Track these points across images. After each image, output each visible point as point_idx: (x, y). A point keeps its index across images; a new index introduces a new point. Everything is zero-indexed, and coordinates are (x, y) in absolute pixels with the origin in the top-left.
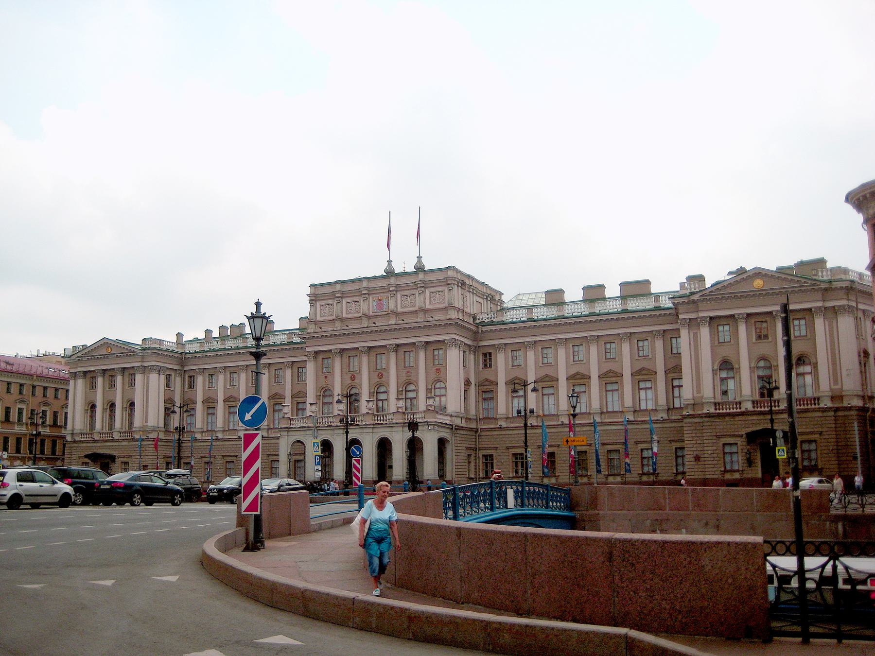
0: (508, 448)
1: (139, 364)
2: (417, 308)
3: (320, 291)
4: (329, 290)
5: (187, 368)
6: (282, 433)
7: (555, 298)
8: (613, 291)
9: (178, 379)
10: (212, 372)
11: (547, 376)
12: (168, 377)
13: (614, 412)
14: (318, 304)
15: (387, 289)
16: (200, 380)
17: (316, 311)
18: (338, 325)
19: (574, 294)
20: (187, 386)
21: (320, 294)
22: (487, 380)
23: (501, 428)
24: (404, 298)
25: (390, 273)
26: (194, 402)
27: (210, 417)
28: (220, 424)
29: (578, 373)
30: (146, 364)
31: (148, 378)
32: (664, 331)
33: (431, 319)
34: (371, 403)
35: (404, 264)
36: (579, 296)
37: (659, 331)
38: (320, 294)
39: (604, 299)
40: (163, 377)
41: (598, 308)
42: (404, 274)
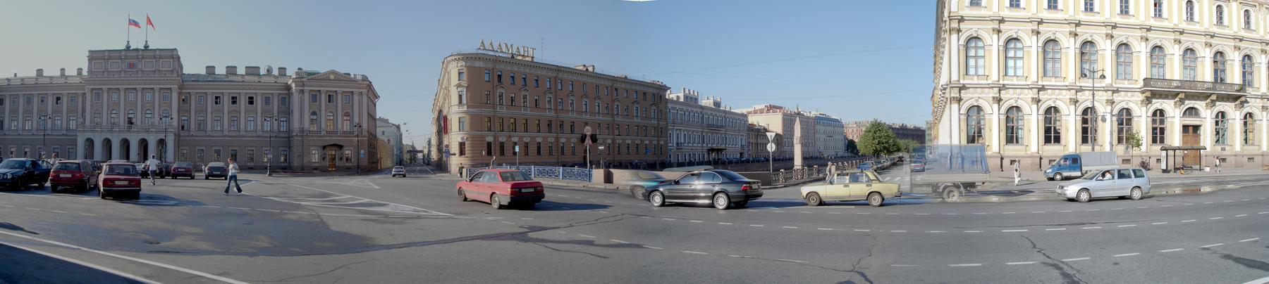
7: (211, 69)
8: (241, 71)
19: (221, 70)
35: (137, 44)
38: (94, 56)
41: (231, 78)
42: (137, 50)
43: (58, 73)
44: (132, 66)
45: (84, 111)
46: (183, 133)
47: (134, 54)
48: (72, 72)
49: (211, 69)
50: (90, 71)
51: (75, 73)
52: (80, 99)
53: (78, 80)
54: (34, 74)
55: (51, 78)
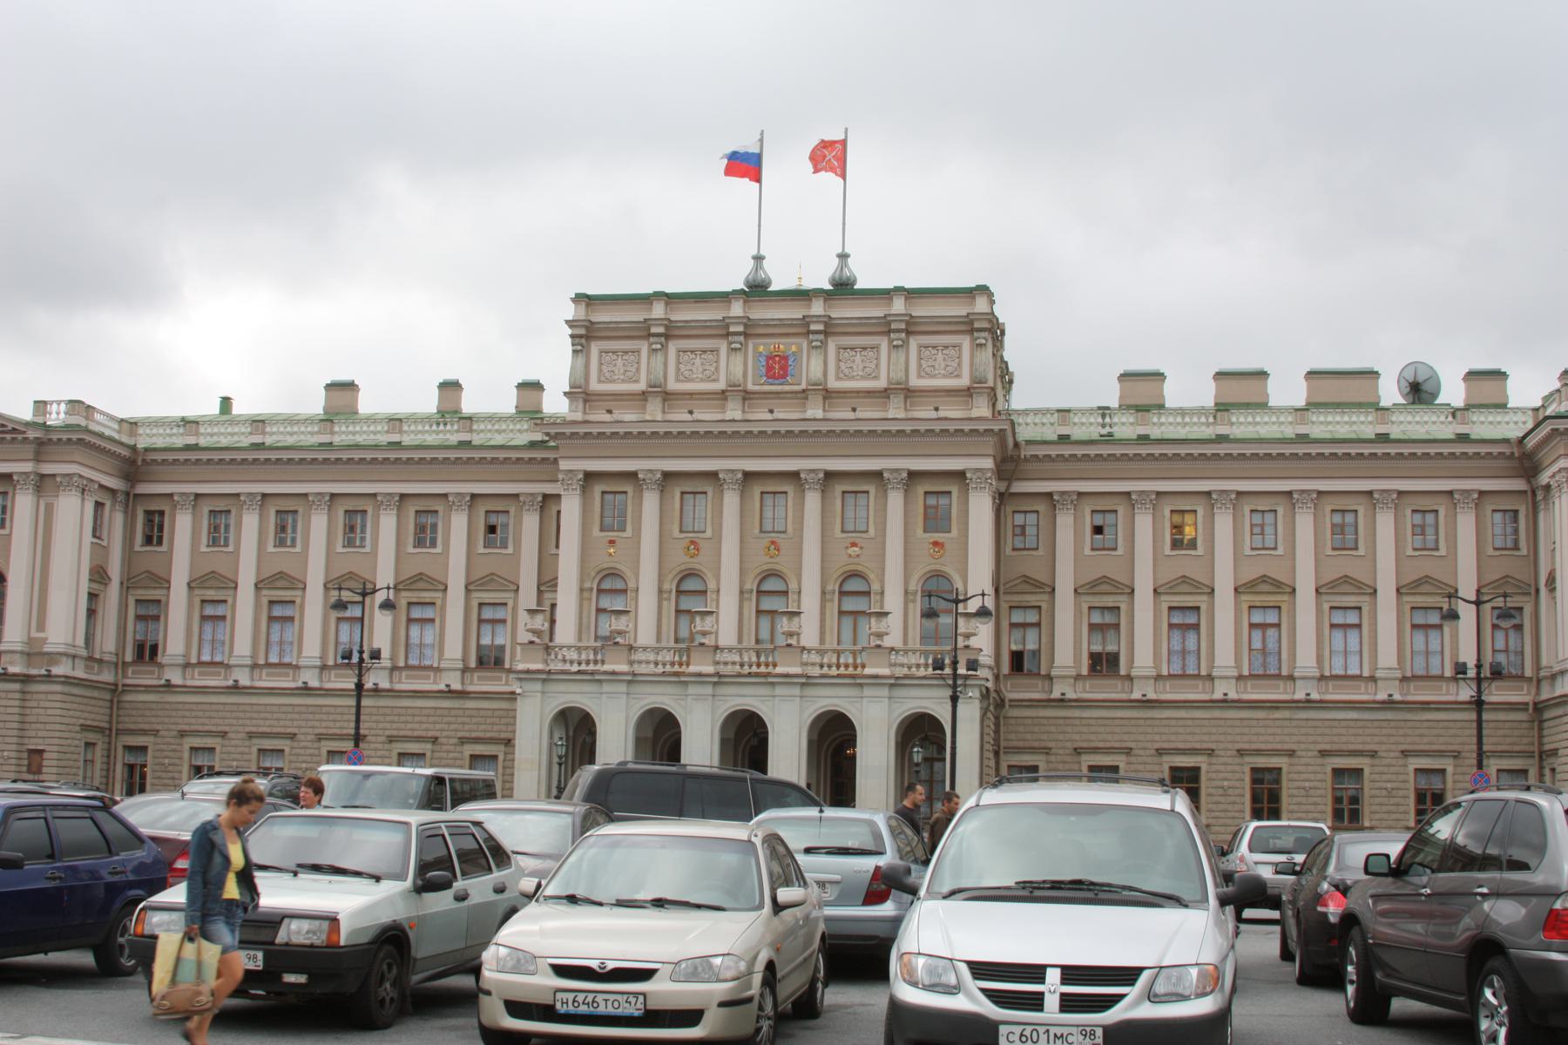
0: (1078, 751)
1: (28, 467)
2: (881, 383)
3: (602, 316)
4: (635, 315)
5: (143, 489)
6: (529, 686)
7: (1142, 387)
8: (1288, 391)
9: (119, 518)
10: (221, 505)
11: (1184, 579)
12: (99, 505)
13: (1346, 677)
14: (595, 348)
15: (803, 328)
16: (182, 527)
17: (587, 366)
18: (654, 411)
19: (1191, 390)
20: (204, 540)
21: (598, 323)
22: (1027, 580)
23: (1062, 702)
24: (846, 355)
25: (757, 290)
26: (164, 582)
27: (276, 627)
28: (243, 647)
29: (1264, 579)
30: (48, 469)
31: (49, 510)
32: (1481, 493)
33: (607, 417)
34: (539, 618)
35: (801, 265)
36: (1206, 395)
37: (1468, 492)
38: (598, 323)
39: (1263, 406)
40: (90, 508)
42: (801, 295)
43: (429, 403)
44: (777, 367)
45: (547, 583)
46: (1016, 691)
47: (793, 312)
48: (490, 397)
49: (1142, 387)
50: (579, 393)
51: (507, 403)
52: (530, 523)
53: (523, 435)
54: (315, 404)
55: (395, 421)
